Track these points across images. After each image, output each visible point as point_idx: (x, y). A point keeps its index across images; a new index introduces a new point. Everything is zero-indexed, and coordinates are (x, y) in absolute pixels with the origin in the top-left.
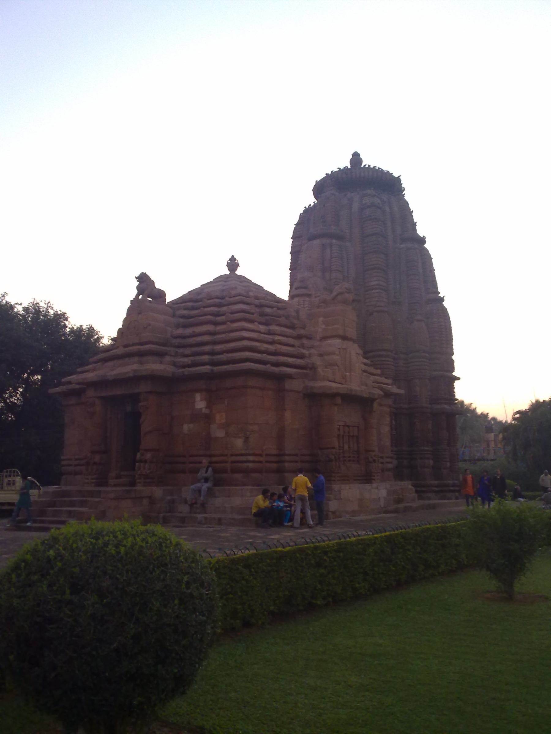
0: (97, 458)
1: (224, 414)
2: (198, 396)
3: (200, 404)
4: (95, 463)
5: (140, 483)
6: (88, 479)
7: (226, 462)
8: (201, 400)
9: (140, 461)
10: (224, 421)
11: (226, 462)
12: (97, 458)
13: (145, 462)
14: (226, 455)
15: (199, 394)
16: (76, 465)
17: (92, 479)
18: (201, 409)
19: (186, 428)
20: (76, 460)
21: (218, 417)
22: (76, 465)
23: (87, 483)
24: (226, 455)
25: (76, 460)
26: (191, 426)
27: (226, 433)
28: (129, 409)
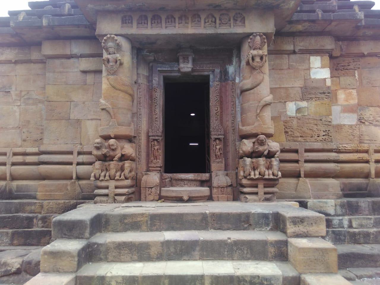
0: (128, 149)
1: (354, 92)
2: (316, 61)
3: (319, 70)
4: (123, 158)
5: (256, 193)
6: (107, 188)
7: (367, 162)
8: (323, 67)
9: (254, 154)
10: (354, 102)
11: (367, 162)
12: (128, 149)
13: (270, 155)
14: (367, 152)
15: (318, 58)
16: (13, 164)
17: (117, 187)
18: (325, 79)
19: (291, 108)
20: (15, 154)
21: (341, 96)
22: (13, 164)
23: (107, 195)
24: (367, 152)
25: (15, 154)
26: (304, 104)
27: (361, 121)
28: (186, 67)
